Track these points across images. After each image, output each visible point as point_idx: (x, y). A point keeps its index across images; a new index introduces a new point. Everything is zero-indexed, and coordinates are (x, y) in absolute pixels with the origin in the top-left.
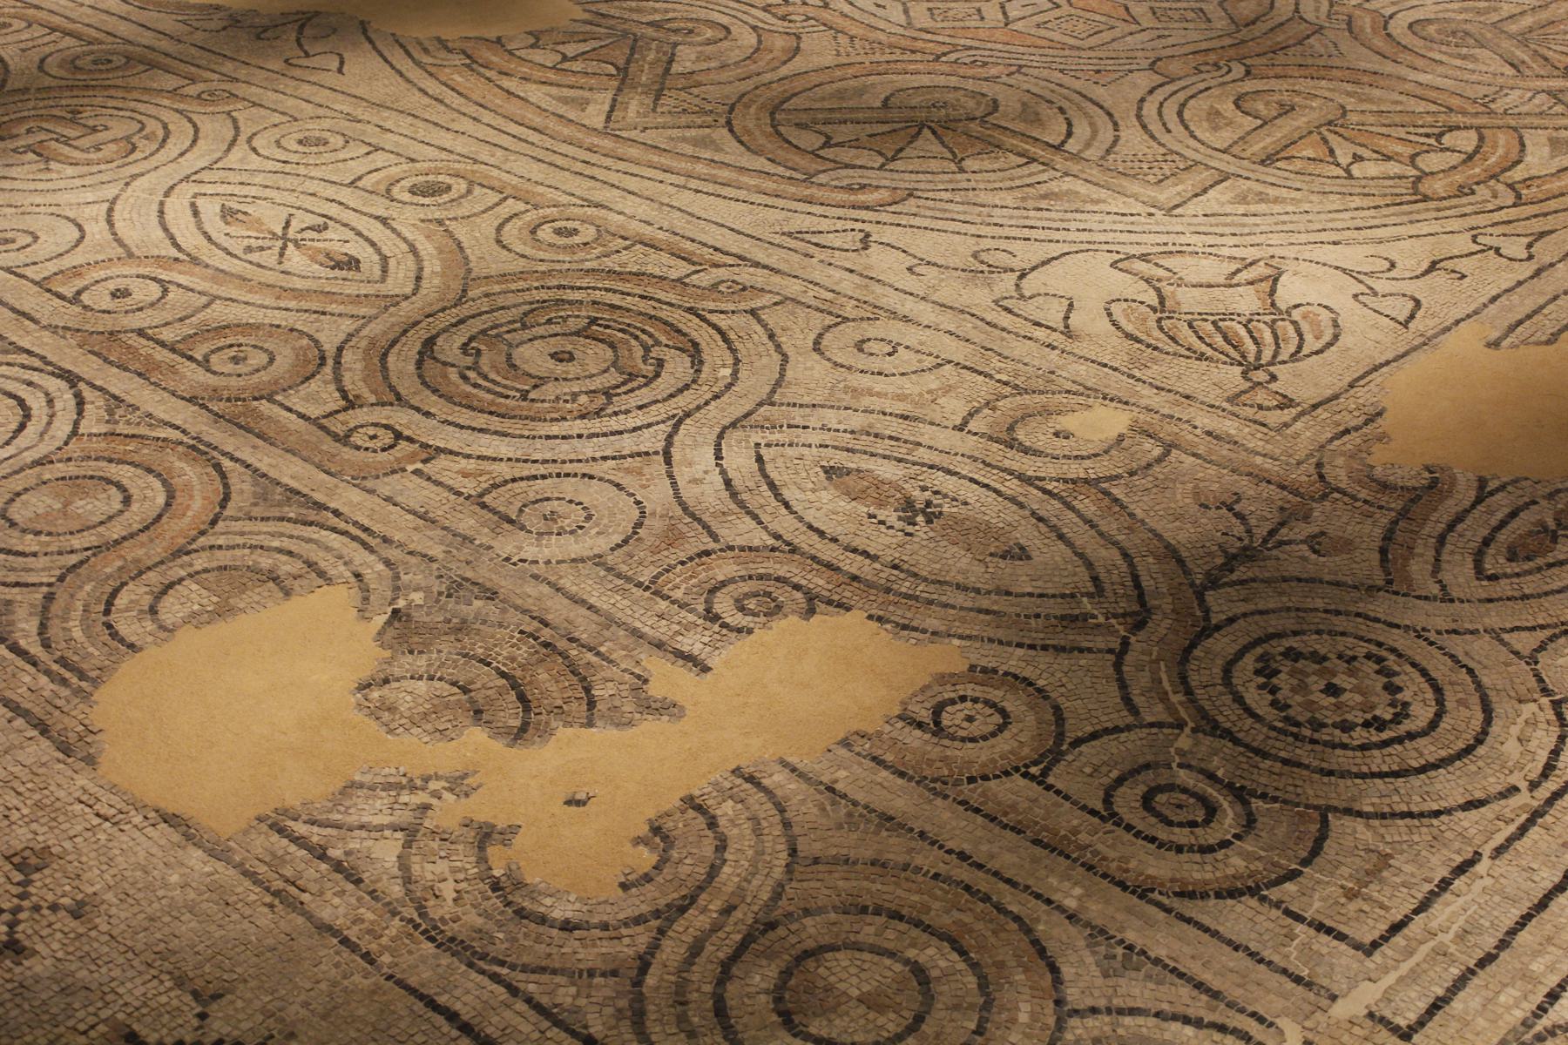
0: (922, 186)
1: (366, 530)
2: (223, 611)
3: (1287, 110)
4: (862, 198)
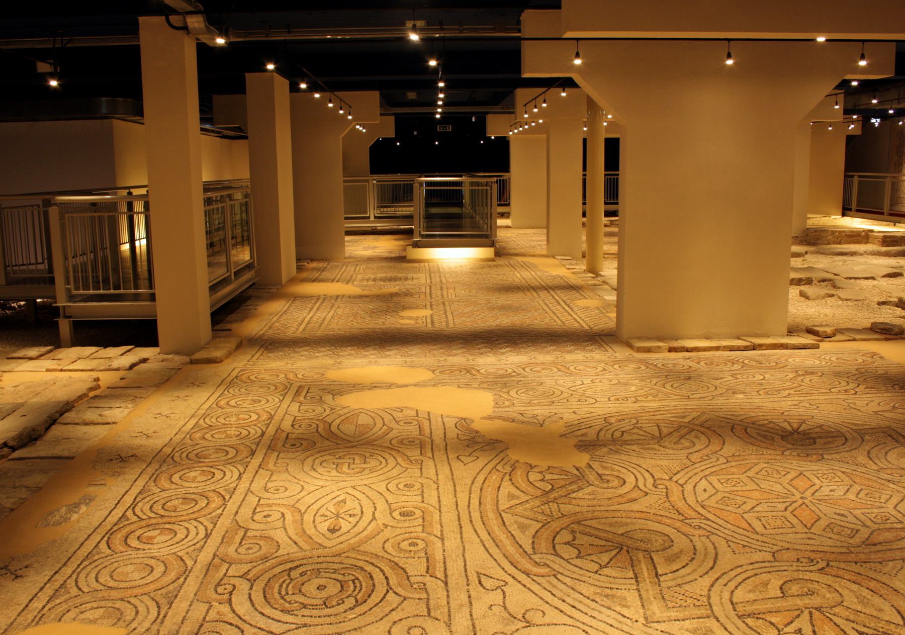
0: (566, 573)
1: (165, 617)
2: (94, 621)
3: (811, 593)
4: (535, 570)
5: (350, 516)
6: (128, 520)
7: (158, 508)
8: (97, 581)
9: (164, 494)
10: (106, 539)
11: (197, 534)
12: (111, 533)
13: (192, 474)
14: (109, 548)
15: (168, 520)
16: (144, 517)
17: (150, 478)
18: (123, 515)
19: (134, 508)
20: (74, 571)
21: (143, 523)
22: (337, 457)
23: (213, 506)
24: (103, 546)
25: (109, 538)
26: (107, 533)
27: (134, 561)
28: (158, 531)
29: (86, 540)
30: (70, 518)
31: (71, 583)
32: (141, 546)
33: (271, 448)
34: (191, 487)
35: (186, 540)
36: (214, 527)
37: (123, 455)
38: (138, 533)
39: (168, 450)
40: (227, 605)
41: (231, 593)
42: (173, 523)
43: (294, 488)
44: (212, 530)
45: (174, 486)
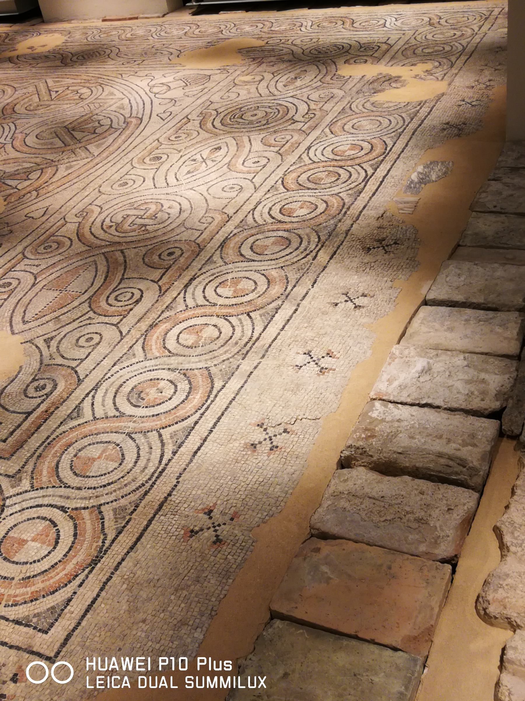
5: (195, 160)
6: (371, 166)
7: (344, 175)
8: (390, 121)
9: (336, 190)
10: (388, 149)
11: (316, 150)
12: (385, 154)
13: (303, 212)
14: (384, 141)
15: (335, 163)
16: (356, 167)
17: (348, 209)
18: (376, 170)
19: (367, 175)
20: (407, 126)
21: (357, 161)
22: (143, 228)
23: (294, 175)
24: (390, 143)
25: (386, 149)
26: (388, 153)
27: (365, 132)
28: (347, 154)
29: (404, 148)
30: (424, 167)
31: (407, 120)
32: (361, 143)
33: (200, 248)
34: (307, 196)
35: (325, 146)
36: (301, 155)
37: (381, 251)
38: (363, 153)
39: (323, 257)
40: (311, 108)
41: (307, 113)
42: (333, 160)
43: (216, 190)
44: (304, 153)
45: (325, 198)
